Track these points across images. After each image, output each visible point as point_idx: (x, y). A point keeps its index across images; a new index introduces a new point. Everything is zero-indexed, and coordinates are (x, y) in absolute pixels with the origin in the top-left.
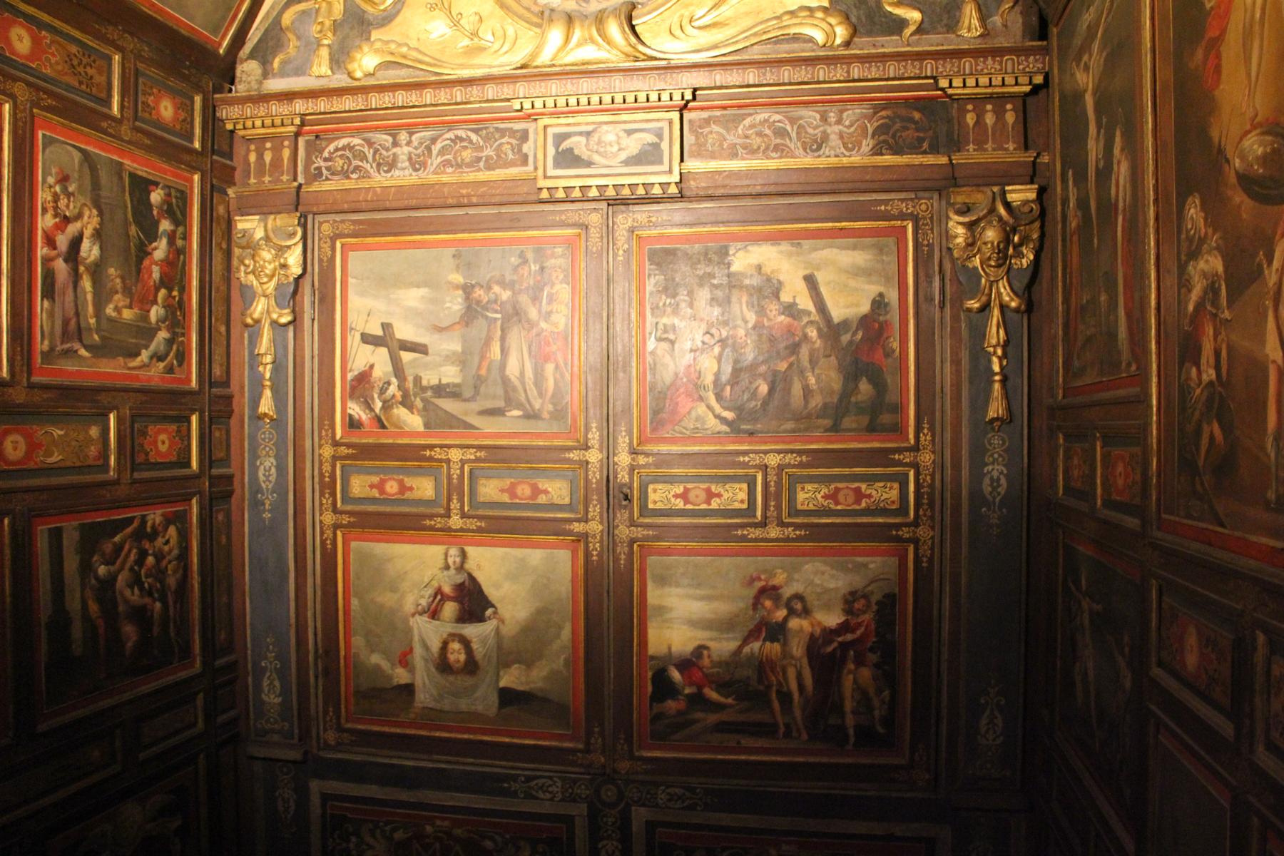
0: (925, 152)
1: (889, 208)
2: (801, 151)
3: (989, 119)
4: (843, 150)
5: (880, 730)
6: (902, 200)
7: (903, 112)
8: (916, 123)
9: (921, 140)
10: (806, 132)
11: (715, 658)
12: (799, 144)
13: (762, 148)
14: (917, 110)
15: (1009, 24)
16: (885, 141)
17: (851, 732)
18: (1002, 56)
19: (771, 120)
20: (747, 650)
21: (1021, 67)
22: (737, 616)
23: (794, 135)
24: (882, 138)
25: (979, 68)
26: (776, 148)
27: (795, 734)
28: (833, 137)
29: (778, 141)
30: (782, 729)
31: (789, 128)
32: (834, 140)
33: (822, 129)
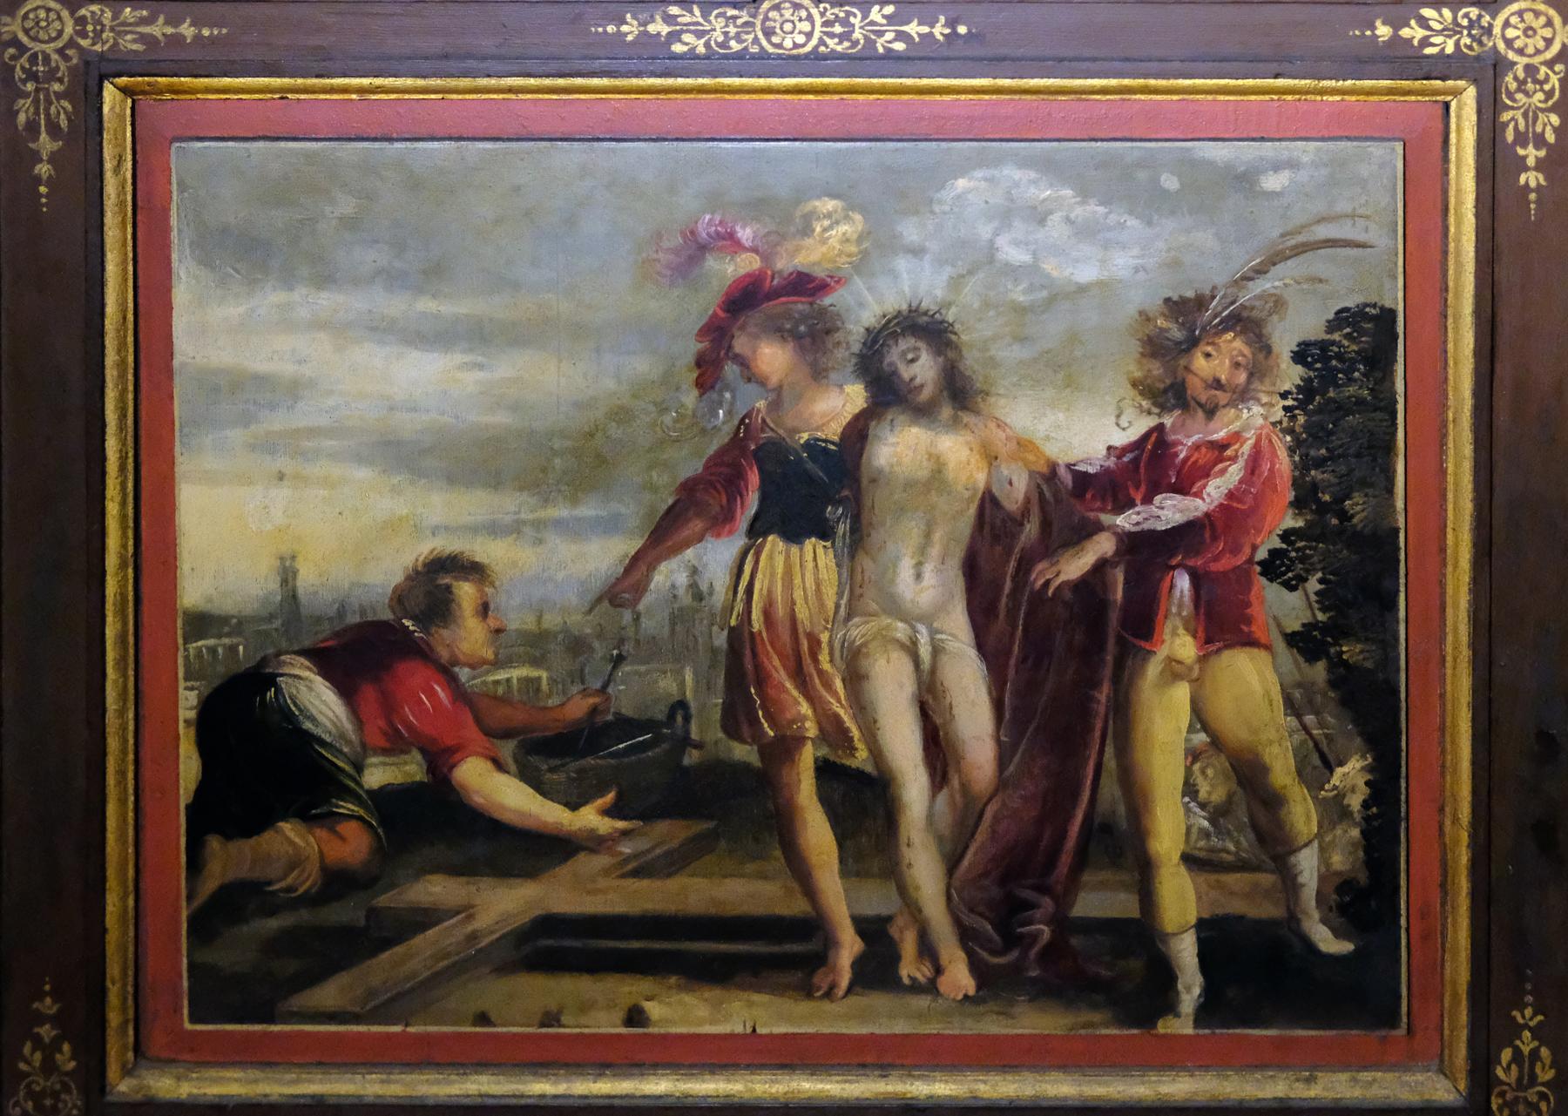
5: (1328, 941)
11: (517, 620)
17: (1186, 951)
20: (670, 575)
22: (622, 415)
27: (910, 968)
30: (849, 946)
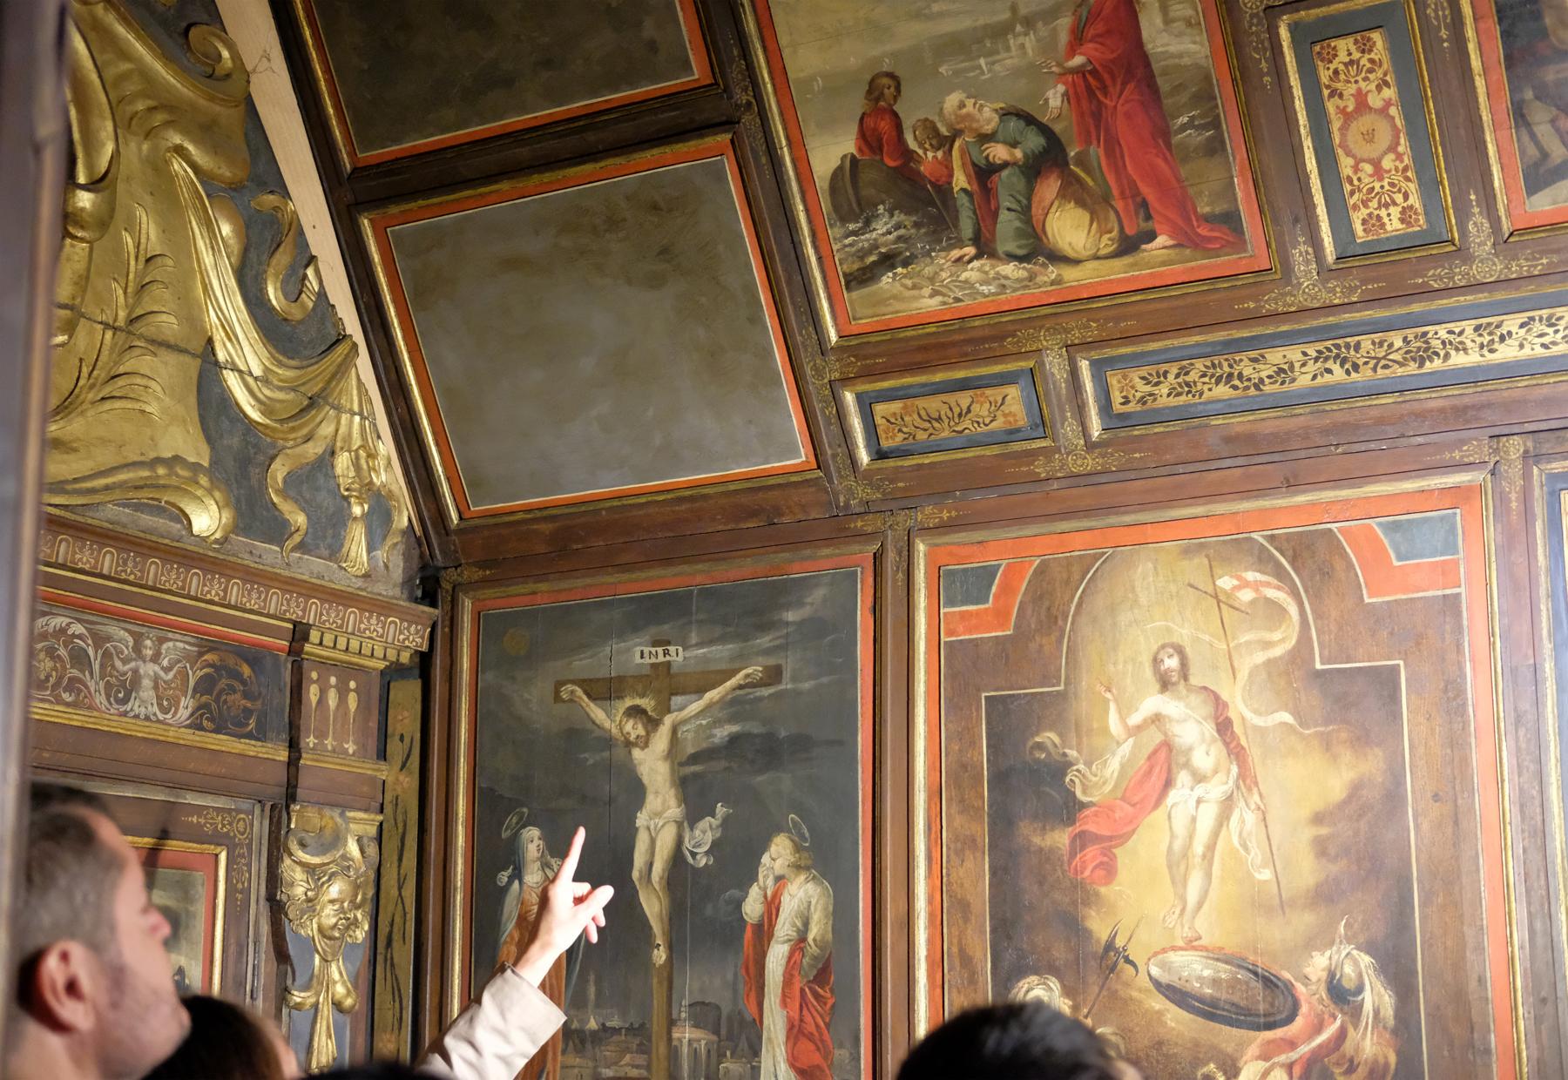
0: (249, 736)
1: (202, 821)
2: (103, 698)
3: (332, 699)
4: (156, 709)
6: (218, 810)
7: (231, 661)
8: (244, 682)
9: (248, 713)
10: (113, 666)
12: (102, 684)
13: (52, 680)
14: (247, 661)
15: (391, 565)
16: (206, 706)
18: (387, 616)
19: (70, 632)
21: (402, 637)
23: (96, 667)
24: (204, 699)
25: (363, 626)
26: (73, 685)
28: (146, 683)
29: (75, 673)
31: (91, 652)
32: (147, 692)
33: (133, 664)
